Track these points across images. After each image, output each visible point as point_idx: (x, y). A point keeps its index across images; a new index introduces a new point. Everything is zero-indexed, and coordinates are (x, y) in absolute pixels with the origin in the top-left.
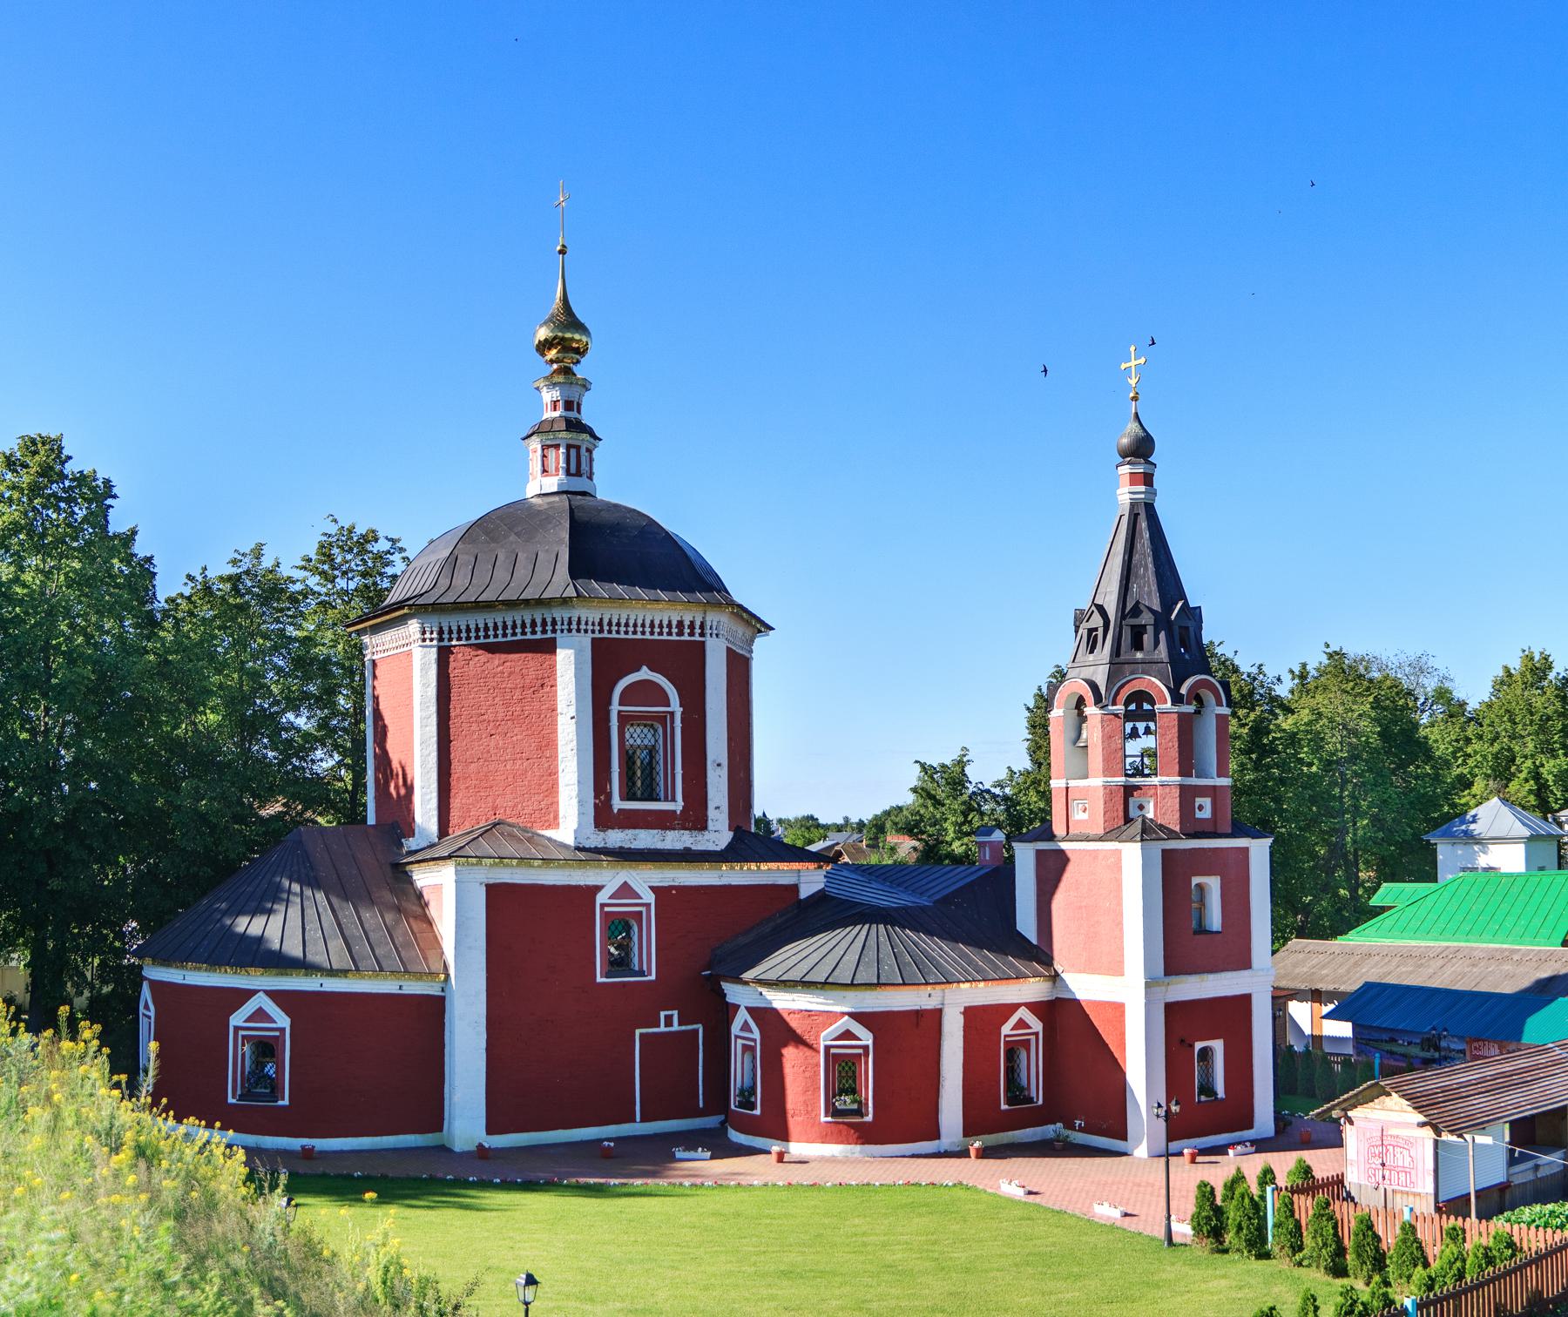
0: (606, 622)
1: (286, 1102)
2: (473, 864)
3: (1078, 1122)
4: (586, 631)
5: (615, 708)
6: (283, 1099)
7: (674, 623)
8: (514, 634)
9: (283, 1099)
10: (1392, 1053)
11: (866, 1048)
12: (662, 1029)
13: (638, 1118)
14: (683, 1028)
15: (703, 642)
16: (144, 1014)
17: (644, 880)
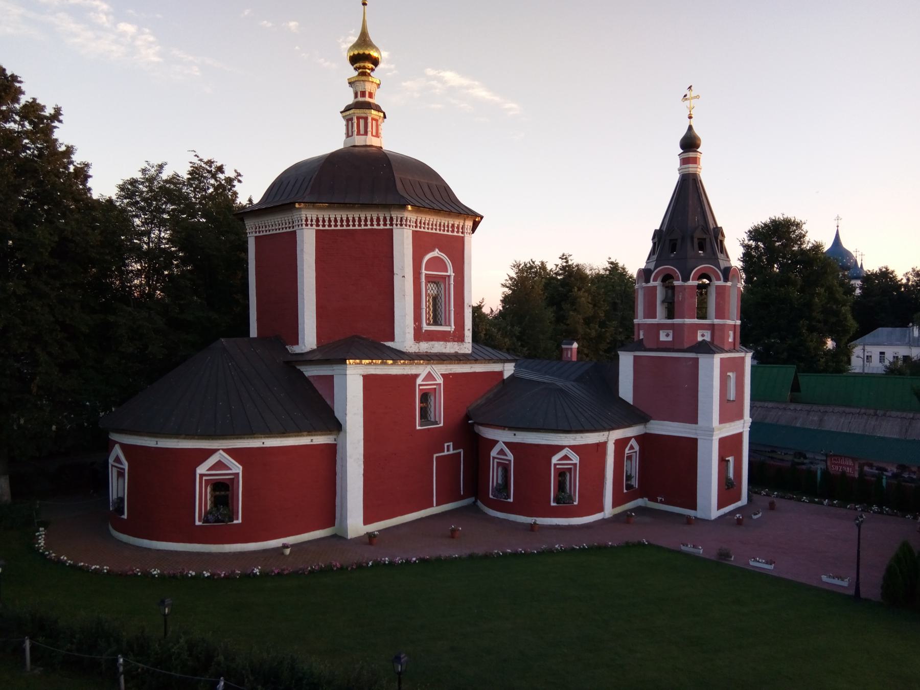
0: (419, 221)
1: (240, 521)
2: (358, 364)
3: (659, 498)
4: (410, 226)
5: (424, 272)
6: (237, 519)
7: (450, 225)
8: (366, 225)
9: (237, 519)
10: (772, 458)
11: (575, 465)
12: (446, 453)
13: (435, 505)
14: (455, 452)
15: (463, 238)
16: (112, 466)
17: (439, 370)
